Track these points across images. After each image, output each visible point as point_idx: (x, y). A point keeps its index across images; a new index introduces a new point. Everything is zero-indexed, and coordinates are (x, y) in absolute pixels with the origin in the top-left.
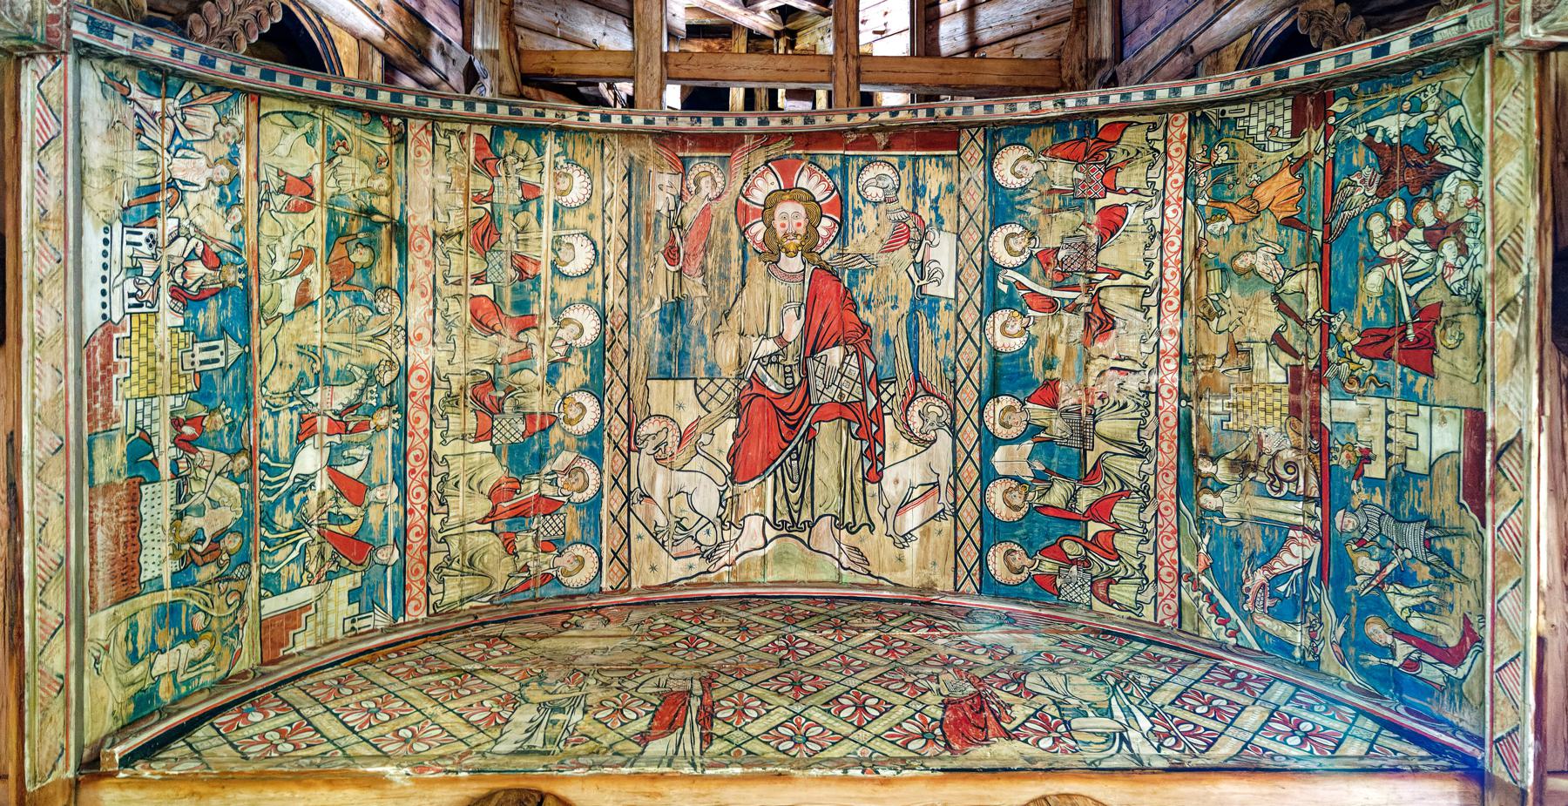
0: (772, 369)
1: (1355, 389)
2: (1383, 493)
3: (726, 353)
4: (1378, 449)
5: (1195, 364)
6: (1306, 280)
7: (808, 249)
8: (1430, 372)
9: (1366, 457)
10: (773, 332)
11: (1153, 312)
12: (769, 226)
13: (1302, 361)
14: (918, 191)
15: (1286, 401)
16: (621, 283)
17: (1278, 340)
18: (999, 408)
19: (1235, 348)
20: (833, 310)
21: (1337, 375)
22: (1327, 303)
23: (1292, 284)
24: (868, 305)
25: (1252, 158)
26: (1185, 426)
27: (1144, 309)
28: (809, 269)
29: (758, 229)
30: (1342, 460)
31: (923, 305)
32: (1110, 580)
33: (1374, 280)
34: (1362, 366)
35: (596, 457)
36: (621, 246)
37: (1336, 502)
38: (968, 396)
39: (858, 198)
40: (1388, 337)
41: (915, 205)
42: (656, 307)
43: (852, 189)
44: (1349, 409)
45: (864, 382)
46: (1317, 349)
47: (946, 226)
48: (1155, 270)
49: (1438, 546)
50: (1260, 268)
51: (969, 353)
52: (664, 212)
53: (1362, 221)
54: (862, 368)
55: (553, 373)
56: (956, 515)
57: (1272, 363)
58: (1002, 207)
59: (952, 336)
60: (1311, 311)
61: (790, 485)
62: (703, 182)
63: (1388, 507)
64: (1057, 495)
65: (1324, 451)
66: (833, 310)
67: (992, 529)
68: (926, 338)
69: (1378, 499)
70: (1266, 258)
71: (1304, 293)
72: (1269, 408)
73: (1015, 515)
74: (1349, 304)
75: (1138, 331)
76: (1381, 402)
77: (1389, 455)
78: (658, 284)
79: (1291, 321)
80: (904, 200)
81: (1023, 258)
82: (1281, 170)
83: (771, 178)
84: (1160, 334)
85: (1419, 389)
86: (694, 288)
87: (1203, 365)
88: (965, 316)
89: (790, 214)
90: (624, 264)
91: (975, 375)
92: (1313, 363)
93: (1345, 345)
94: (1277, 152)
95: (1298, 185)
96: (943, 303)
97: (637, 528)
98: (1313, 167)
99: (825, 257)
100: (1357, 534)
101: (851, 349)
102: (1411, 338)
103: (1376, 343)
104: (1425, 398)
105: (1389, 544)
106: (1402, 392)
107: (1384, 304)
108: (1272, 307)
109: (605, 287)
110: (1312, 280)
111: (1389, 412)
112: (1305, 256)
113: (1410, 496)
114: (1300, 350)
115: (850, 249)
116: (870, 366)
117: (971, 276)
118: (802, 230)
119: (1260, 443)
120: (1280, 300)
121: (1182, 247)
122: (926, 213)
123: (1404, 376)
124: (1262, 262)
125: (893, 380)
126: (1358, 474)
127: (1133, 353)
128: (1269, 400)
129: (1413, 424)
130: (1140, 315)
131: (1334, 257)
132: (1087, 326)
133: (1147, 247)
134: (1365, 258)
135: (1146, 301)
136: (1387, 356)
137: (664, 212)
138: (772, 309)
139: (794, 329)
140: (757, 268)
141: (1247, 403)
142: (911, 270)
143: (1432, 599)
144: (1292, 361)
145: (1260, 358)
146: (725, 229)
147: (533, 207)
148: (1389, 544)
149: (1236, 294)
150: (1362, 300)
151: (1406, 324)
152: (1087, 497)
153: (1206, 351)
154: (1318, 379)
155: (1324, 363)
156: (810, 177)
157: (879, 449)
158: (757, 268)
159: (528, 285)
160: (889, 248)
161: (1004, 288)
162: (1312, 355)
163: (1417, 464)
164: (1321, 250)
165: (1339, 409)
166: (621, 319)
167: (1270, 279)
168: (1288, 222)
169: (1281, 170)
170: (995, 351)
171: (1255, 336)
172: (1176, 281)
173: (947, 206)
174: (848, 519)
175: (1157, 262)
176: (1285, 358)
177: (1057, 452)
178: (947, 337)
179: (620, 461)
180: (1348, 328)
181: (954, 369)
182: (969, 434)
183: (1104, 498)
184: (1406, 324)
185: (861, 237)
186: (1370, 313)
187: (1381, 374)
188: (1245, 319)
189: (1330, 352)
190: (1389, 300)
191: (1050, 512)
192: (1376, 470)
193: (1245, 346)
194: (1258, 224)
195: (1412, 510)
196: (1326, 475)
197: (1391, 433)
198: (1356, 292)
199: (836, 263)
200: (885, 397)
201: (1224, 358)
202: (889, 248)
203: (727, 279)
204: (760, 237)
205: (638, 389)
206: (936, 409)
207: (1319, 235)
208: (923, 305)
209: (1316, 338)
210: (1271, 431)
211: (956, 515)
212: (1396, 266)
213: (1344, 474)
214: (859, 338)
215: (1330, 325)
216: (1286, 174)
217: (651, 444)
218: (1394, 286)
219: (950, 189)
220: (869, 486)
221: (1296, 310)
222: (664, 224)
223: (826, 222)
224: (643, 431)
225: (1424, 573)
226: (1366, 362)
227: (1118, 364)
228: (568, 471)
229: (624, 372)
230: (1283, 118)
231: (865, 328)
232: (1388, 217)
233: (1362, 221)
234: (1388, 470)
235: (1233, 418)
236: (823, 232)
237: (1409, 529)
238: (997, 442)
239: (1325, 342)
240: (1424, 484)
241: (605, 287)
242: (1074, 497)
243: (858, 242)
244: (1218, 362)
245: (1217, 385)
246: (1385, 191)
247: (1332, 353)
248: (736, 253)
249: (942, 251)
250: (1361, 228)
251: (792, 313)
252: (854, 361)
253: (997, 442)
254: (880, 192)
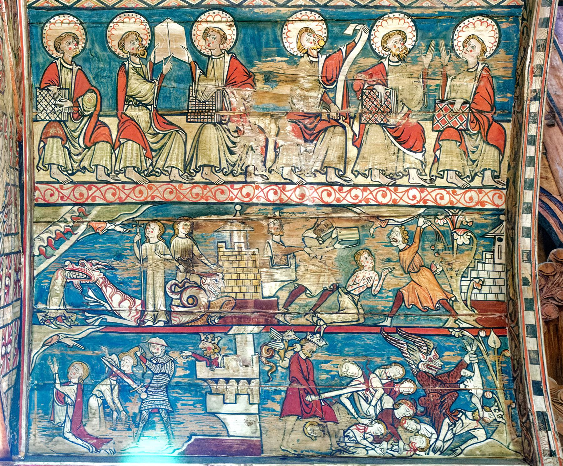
1: (264, 354)
2: (185, 376)
4: (219, 373)
5: (274, 217)
6: (349, 311)
8: (283, 414)
9: (211, 364)
11: (321, 178)
13: (283, 310)
15: (248, 297)
17: (299, 290)
19: (290, 253)
21: (273, 340)
22: (330, 331)
23: (346, 301)
25: (456, 267)
26: (219, 209)
27: (324, 170)
30: (205, 344)
32: (66, 139)
33: (353, 370)
34: (283, 360)
37: (171, 338)
40: (307, 380)
44: (248, 351)
46: (294, 322)
48: (360, 180)
49: (156, 419)
50: (361, 274)
53: (399, 359)
57: (279, 285)
60: (324, 316)
63: (175, 380)
65: (210, 328)
69: (180, 372)
70: (369, 279)
71: (340, 310)
72: (240, 283)
73: (114, 44)
74: (331, 349)
75: (303, 164)
76: (256, 375)
77: (216, 381)
79: (314, 301)
82: (444, 291)
84: (300, 185)
85: (269, 404)
87: (274, 225)
92: (281, 318)
93: (298, 346)
94: (460, 288)
95: (430, 305)
98: (444, 318)
100: (149, 356)
102: (308, 398)
103: (302, 371)
104: (264, 409)
105: (148, 381)
106: (265, 391)
107: (333, 377)
108: (327, 285)
110: (349, 318)
111: (249, 381)
112: (371, 312)
113: (188, 398)
114: (292, 308)
119: (210, 275)
120: (333, 291)
121: (380, 205)
123: (279, 392)
124: (366, 276)
126: (198, 357)
127: (283, 160)
128: (247, 282)
129: (243, 399)
130: (318, 166)
131: (370, 336)
132: (308, 116)
133: (382, 172)
134: (368, 363)
135: (331, 172)
136: (293, 380)
141: (243, 264)
143: (115, 414)
144: (282, 302)
145: (282, 275)
148: (148, 381)
149: (337, 253)
150: (336, 360)
151: (319, 394)
152: (142, 116)
153: (286, 227)
154: (269, 323)
155: (283, 328)
162: (288, 318)
163: (213, 402)
164: (375, 325)
165: (246, 338)
167: (350, 282)
168: (399, 298)
169: (444, 291)
171: (302, 270)
172: (349, 200)
175: (368, 181)
176: (284, 296)
177: (182, 86)
180: (312, 348)
183: (143, 134)
184: (319, 394)
186: (325, 366)
187: (278, 375)
188: (316, 261)
189: (291, 333)
190: (337, 381)
191: (122, 79)
192: (202, 371)
193: (292, 261)
194: (398, 272)
195: (177, 399)
196: (192, 331)
197: (233, 382)
198: (341, 354)
201: (280, 243)
207: (387, 323)
209: (302, 321)
210: (221, 284)
212: (363, 387)
213: (195, 345)
215: (313, 333)
216: (440, 296)
218: (348, 385)
221: (325, 304)
225: (133, 408)
226: (286, 363)
227: (271, 146)
230: (488, 293)
232: (401, 380)
233: (399, 359)
234: (205, 380)
235: (228, 252)
237: (161, 396)
239: (299, 329)
240: (199, 409)
244: (277, 238)
245: (256, 237)
246: (421, 377)
247: (291, 335)
250: (393, 358)
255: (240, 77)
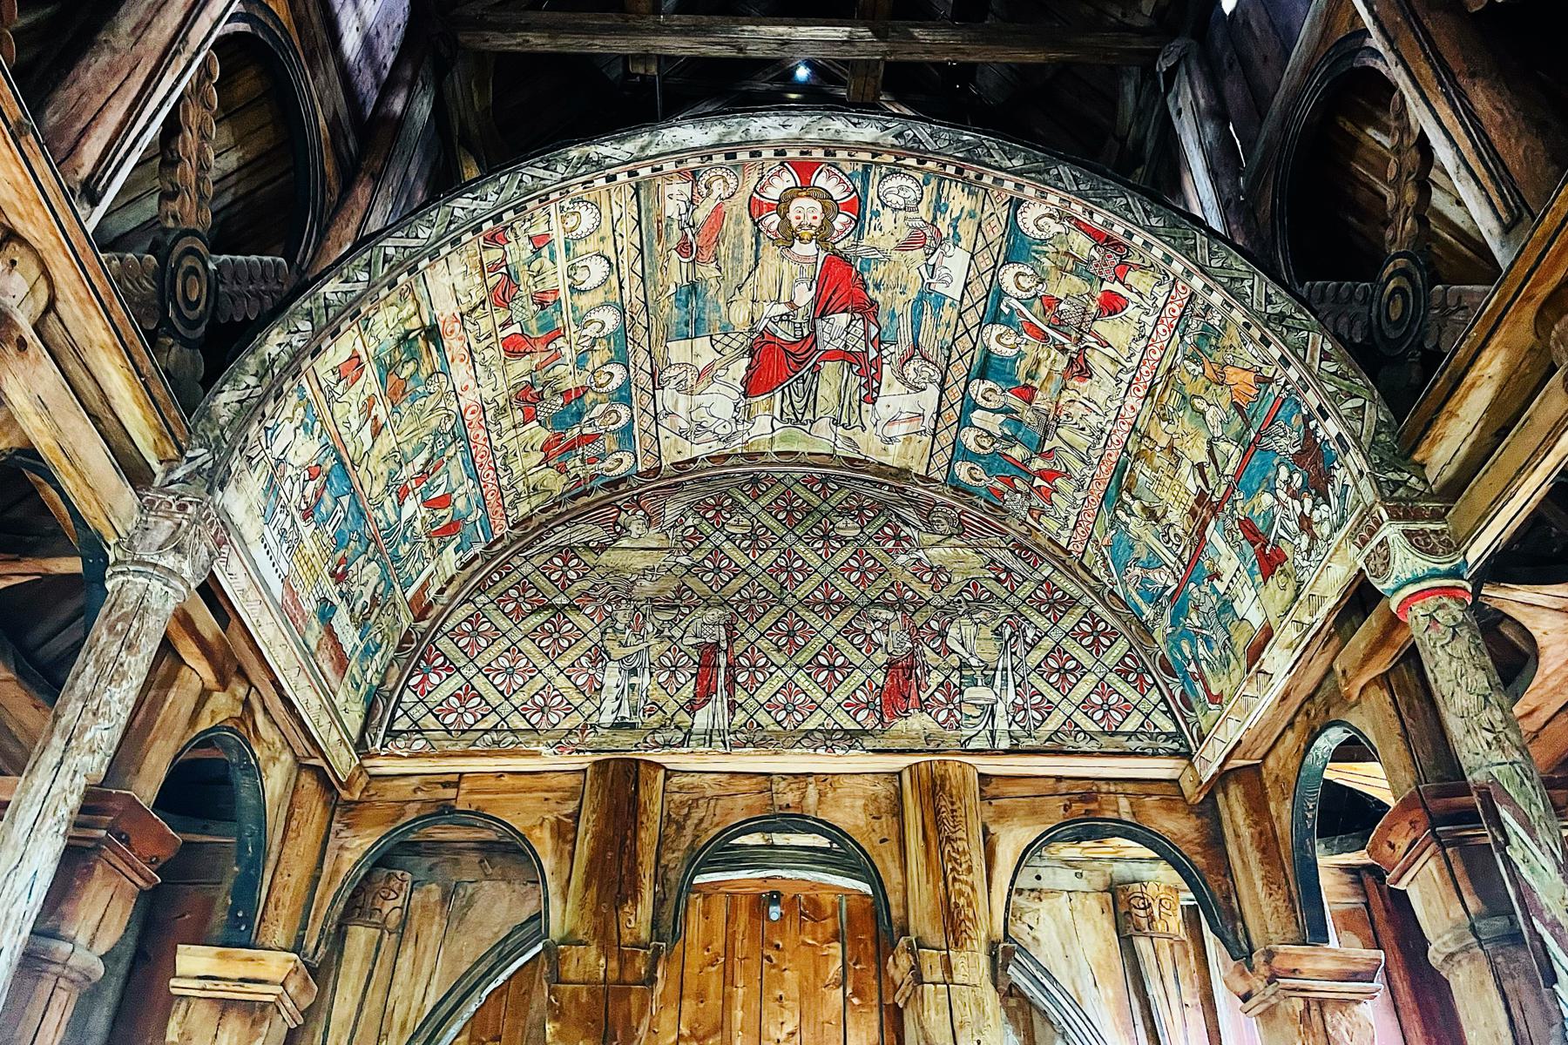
0: (783, 325)
3: (739, 315)
7: (822, 236)
10: (785, 298)
12: (783, 217)
14: (939, 207)
16: (637, 280)
18: (983, 387)
20: (842, 284)
24: (877, 286)
28: (822, 255)
29: (773, 220)
31: (927, 299)
35: (627, 401)
36: (634, 253)
38: (958, 371)
39: (877, 201)
41: (935, 218)
42: (673, 289)
43: (872, 193)
45: (868, 341)
47: (963, 244)
51: (965, 343)
52: (675, 216)
54: (866, 332)
55: (580, 362)
56: (934, 436)
58: (1016, 247)
59: (953, 327)
61: (795, 398)
62: (714, 186)
64: (1018, 452)
66: (842, 284)
67: (960, 451)
68: (928, 321)
78: (676, 272)
80: (924, 211)
81: (1029, 294)
83: (786, 176)
86: (708, 272)
88: (967, 316)
89: (806, 210)
90: (638, 267)
91: (967, 358)
96: (948, 301)
97: (663, 433)
99: (839, 246)
101: (858, 316)
109: (621, 288)
115: (864, 242)
116: (874, 331)
117: (979, 290)
118: (817, 223)
122: (943, 226)
125: (895, 343)
137: (675, 216)
138: (781, 285)
139: (804, 296)
140: (770, 253)
142: (923, 269)
146: (738, 222)
147: (545, 252)
156: (829, 178)
157: (875, 384)
158: (770, 253)
159: (550, 310)
160: (903, 247)
161: (1007, 311)
166: (639, 306)
170: (988, 353)
173: (967, 228)
174: (845, 420)
178: (948, 326)
179: (646, 398)
181: (950, 349)
182: (954, 393)
185: (878, 234)
199: (851, 253)
200: (885, 353)
202: (903, 247)
203: (741, 261)
204: (774, 227)
205: (658, 351)
206: (929, 370)
208: (927, 299)
211: (934, 436)
214: (867, 310)
217: (673, 382)
219: (972, 215)
220: (864, 405)
222: (675, 226)
223: (842, 218)
224: (666, 375)
228: (603, 415)
229: (645, 343)
231: (873, 303)
236: (837, 225)
238: (976, 407)
241: (621, 288)
242: (1030, 460)
243: (871, 237)
248: (748, 239)
249: (955, 263)
251: (804, 286)
252: (860, 325)
253: (976, 407)
254: (901, 201)
255: (1027, 393)
